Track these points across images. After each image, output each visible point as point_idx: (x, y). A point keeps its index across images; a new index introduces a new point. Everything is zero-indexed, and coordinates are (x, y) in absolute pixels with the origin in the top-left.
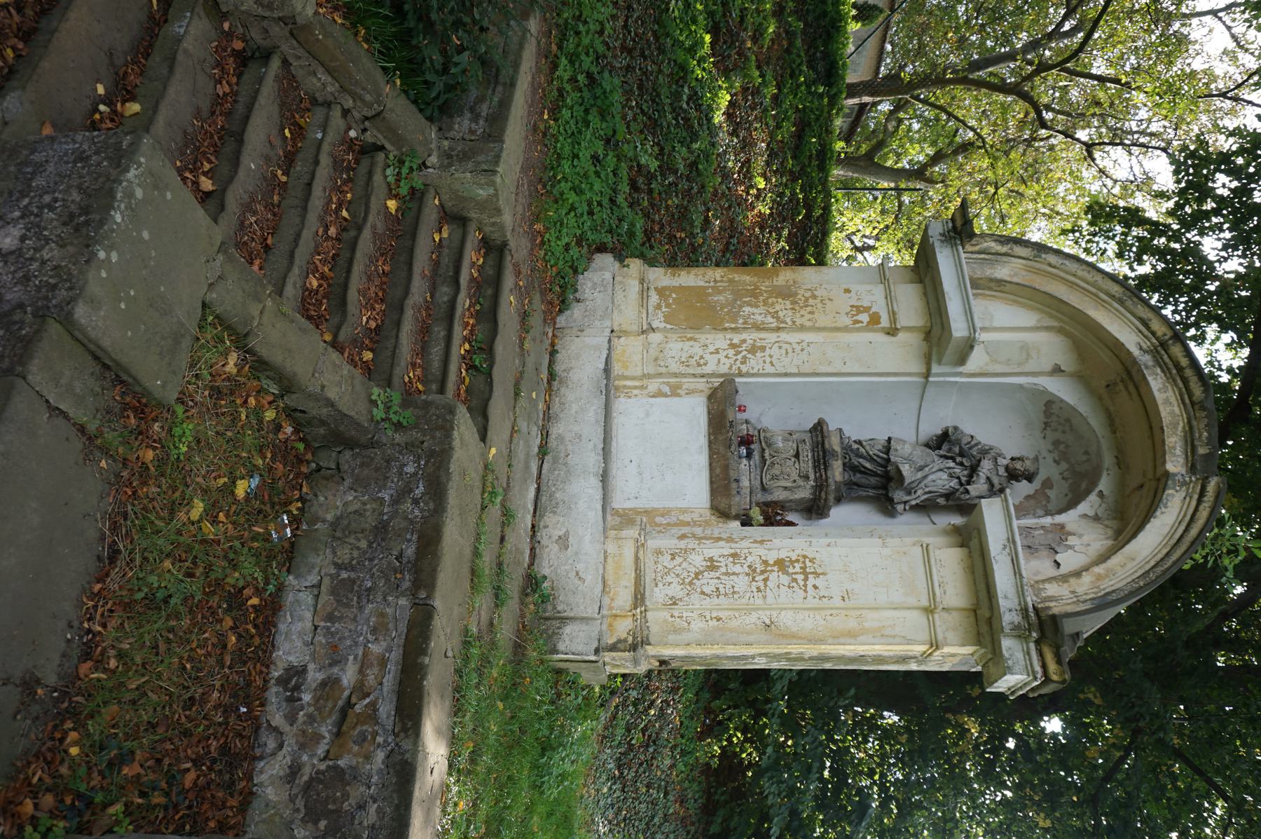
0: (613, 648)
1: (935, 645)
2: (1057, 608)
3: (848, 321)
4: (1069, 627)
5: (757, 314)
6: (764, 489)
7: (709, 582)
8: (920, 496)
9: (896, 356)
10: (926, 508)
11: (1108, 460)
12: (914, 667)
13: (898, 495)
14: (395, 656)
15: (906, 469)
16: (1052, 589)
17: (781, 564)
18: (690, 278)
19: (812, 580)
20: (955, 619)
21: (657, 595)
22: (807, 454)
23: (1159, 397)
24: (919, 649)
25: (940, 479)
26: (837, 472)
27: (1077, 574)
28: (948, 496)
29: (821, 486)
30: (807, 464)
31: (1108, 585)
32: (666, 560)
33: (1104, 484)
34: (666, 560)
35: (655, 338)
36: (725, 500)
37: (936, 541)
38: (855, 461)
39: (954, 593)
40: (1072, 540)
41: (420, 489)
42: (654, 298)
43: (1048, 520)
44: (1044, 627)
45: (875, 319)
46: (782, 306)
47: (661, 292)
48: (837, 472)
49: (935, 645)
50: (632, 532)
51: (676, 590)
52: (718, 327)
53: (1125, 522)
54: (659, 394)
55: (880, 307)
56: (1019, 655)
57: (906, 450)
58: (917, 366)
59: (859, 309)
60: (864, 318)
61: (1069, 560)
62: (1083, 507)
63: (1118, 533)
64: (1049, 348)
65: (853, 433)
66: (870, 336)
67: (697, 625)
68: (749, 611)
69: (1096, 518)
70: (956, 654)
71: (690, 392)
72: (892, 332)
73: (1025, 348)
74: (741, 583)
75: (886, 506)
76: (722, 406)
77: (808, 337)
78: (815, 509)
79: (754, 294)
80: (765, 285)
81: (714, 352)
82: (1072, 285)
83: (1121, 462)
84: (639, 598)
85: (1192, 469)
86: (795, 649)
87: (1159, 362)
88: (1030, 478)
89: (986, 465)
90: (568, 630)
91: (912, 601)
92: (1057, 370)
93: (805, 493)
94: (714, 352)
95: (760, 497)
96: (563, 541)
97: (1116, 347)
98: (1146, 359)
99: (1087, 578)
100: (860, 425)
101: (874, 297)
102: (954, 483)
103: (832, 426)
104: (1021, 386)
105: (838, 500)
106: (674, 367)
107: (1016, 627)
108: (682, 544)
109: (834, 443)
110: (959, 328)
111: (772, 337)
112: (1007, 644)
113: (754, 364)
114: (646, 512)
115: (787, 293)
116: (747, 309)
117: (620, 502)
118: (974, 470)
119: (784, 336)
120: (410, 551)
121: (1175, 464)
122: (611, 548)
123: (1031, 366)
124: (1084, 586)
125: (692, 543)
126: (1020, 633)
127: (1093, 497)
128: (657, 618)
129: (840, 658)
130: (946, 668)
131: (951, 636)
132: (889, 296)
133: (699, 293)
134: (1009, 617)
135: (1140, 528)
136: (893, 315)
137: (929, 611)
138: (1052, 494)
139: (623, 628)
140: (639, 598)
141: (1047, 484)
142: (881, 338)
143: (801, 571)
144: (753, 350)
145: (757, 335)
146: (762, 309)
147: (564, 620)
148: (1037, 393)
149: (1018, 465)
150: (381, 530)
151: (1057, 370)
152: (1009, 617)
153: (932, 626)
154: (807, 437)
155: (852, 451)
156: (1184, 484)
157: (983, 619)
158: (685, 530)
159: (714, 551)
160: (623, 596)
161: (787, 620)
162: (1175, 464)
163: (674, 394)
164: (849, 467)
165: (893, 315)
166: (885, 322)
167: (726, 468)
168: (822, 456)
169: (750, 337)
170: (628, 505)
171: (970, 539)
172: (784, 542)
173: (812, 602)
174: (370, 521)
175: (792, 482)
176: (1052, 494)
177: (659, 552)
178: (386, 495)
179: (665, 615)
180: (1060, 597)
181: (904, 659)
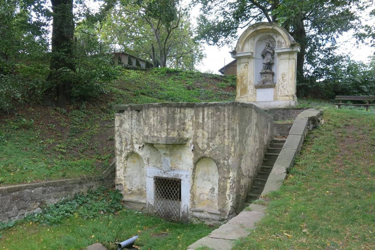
0: (294, 99)
1: (294, 59)
2: (290, 44)
3: (246, 69)
4: (292, 43)
5: (245, 82)
6: (270, 81)
7: (285, 87)
8: (272, 59)
9: (252, 63)
10: (273, 58)
11: (268, 34)
12: (296, 61)
13: (272, 62)
14: (296, 111)
15: (268, 61)
16: (287, 44)
17: (283, 78)
18: (238, 91)
19: (285, 74)
20: (290, 56)
21: (287, 94)
22: (266, 75)
23: (261, 28)
24: (294, 60)
25: (269, 57)
26: (268, 71)
27: (285, 41)
28: (272, 55)
29: (270, 73)
30: (267, 75)
31: (287, 37)
32: (282, 93)
33: (271, 34)
34: (282, 93)
35: (248, 96)
36: (273, 86)
37: (280, 58)
38: (266, 68)
39: (287, 56)
40: (280, 40)
41: (279, 111)
42: (242, 96)
43: (277, 43)
44: (292, 46)
45: (246, 65)
46: (244, 78)
47: (241, 95)
48: (268, 71)
49: (294, 59)
50: (278, 98)
51: (286, 91)
52: (247, 87)
53: (277, 33)
54: (256, 96)
55: (245, 64)
56: (295, 49)
57: (265, 61)
58: (253, 60)
59: (245, 67)
60: (246, 67)
61: (283, 41)
62: (275, 38)
63: (279, 34)
64: (251, 41)
65: (262, 68)
66: (249, 66)
67: (291, 88)
68: (289, 82)
69: (276, 36)
70: (295, 56)
71: (256, 91)
72: (248, 63)
73: (251, 44)
74: (285, 83)
75: (273, 64)
76: (257, 87)
77: (249, 75)
78: (273, 74)
79: (242, 82)
80: (240, 81)
81: (250, 88)
82: (243, 38)
83: (268, 32)
84: (287, 96)
85: (271, 25)
86: (294, 76)
87: (256, 28)
88: (269, 44)
89: (268, 50)
90: (291, 105)
91: (288, 61)
92: (254, 40)
93: (271, 75)
94: (250, 88)
95: (272, 81)
96: (279, 106)
97: (253, 33)
98: (255, 29)
99: (286, 40)
100: (261, 68)
101: (242, 66)
102: (270, 55)
103: (261, 72)
104: (256, 45)
105: (272, 71)
106: (252, 94)
107: (292, 49)
108: (279, 91)
109: (264, 71)
110: (250, 54)
111: (248, 80)
112: (294, 50)
113: (252, 82)
114: (274, 97)
115: (242, 77)
116: (244, 83)
117: (273, 100)
118: (268, 52)
119: (248, 78)
120: (286, 111)
121: (271, 27)
122: (280, 100)
123: (253, 43)
124: (287, 40)
125: (279, 90)
126: (293, 49)
127: (273, 36)
128: (290, 94)
129: (295, 70)
130: (297, 56)
131: (293, 56)
132: (243, 63)
133: (241, 90)
134: (291, 50)
135: (278, 31)
136: (247, 62)
137: (289, 59)
138: (271, 41)
139: (291, 98)
140: (287, 96)
141: (270, 41)
142: (249, 65)
143: (283, 76)
144: (250, 82)
145: (248, 82)
146: (244, 81)
147: (290, 105)
148: (257, 42)
149: (268, 46)
150: (283, 114)
151: (254, 40)
152: (291, 50)
153: (292, 59)
154: (263, 75)
155: (265, 68)
156: (273, 27)
157: (290, 53)
158: (277, 91)
159: (281, 87)
160: (287, 98)
161: (290, 77)
162: (271, 27)
163: (256, 94)
164: (267, 69)
165: (246, 63)
166: (247, 64)
167: (268, 86)
168: (267, 73)
169: (248, 83)
170: (273, 99)
171: (279, 54)
172: (278, 78)
173: (288, 74)
174: (282, 115)
175: (269, 77)
176: (271, 41)
177: (281, 94)
178: (280, 114)
179: (289, 93)
180: (288, 43)
181: (295, 62)
